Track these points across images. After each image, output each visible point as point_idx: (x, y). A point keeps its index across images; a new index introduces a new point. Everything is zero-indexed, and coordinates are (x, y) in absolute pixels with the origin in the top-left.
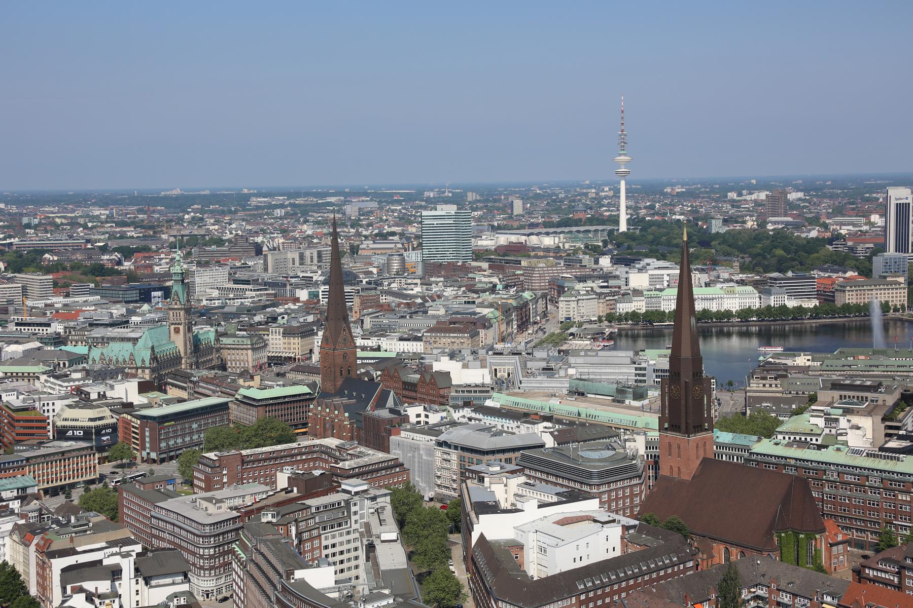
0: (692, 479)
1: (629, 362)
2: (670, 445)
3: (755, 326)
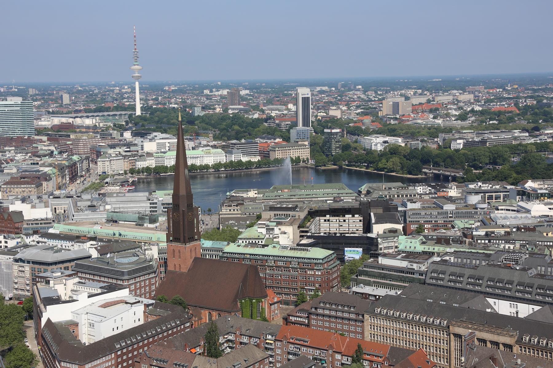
1: (145, 199)
2: (174, 251)
3: (223, 173)
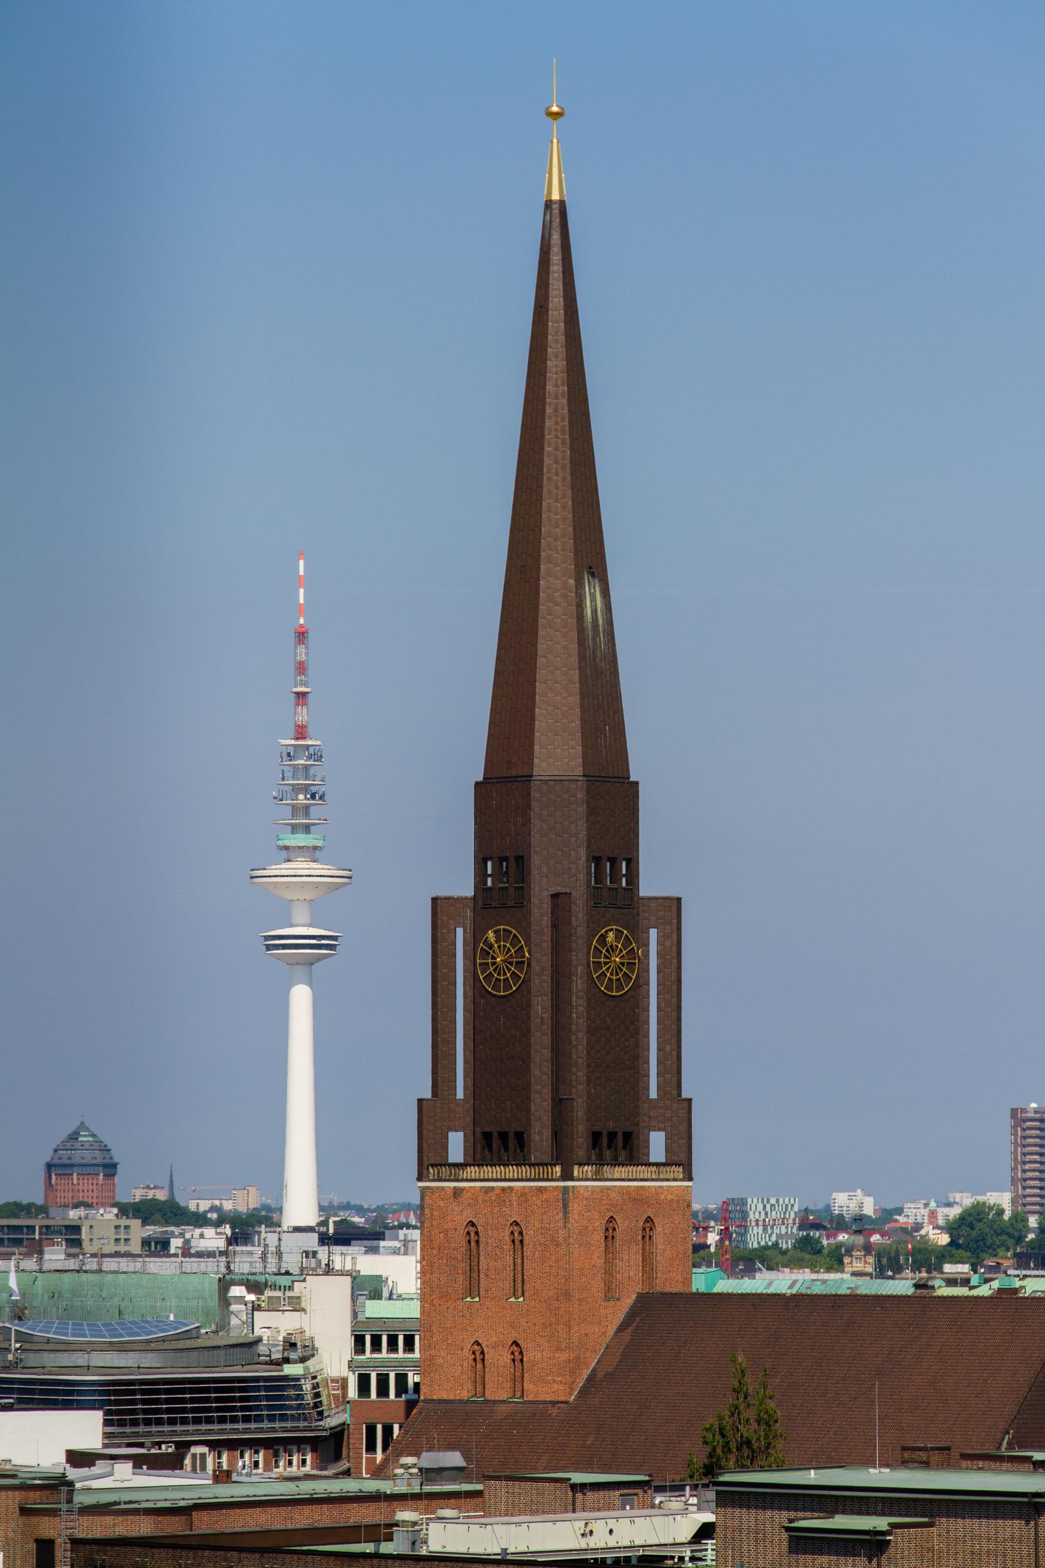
0: (583, 1392)
2: (473, 1231)
